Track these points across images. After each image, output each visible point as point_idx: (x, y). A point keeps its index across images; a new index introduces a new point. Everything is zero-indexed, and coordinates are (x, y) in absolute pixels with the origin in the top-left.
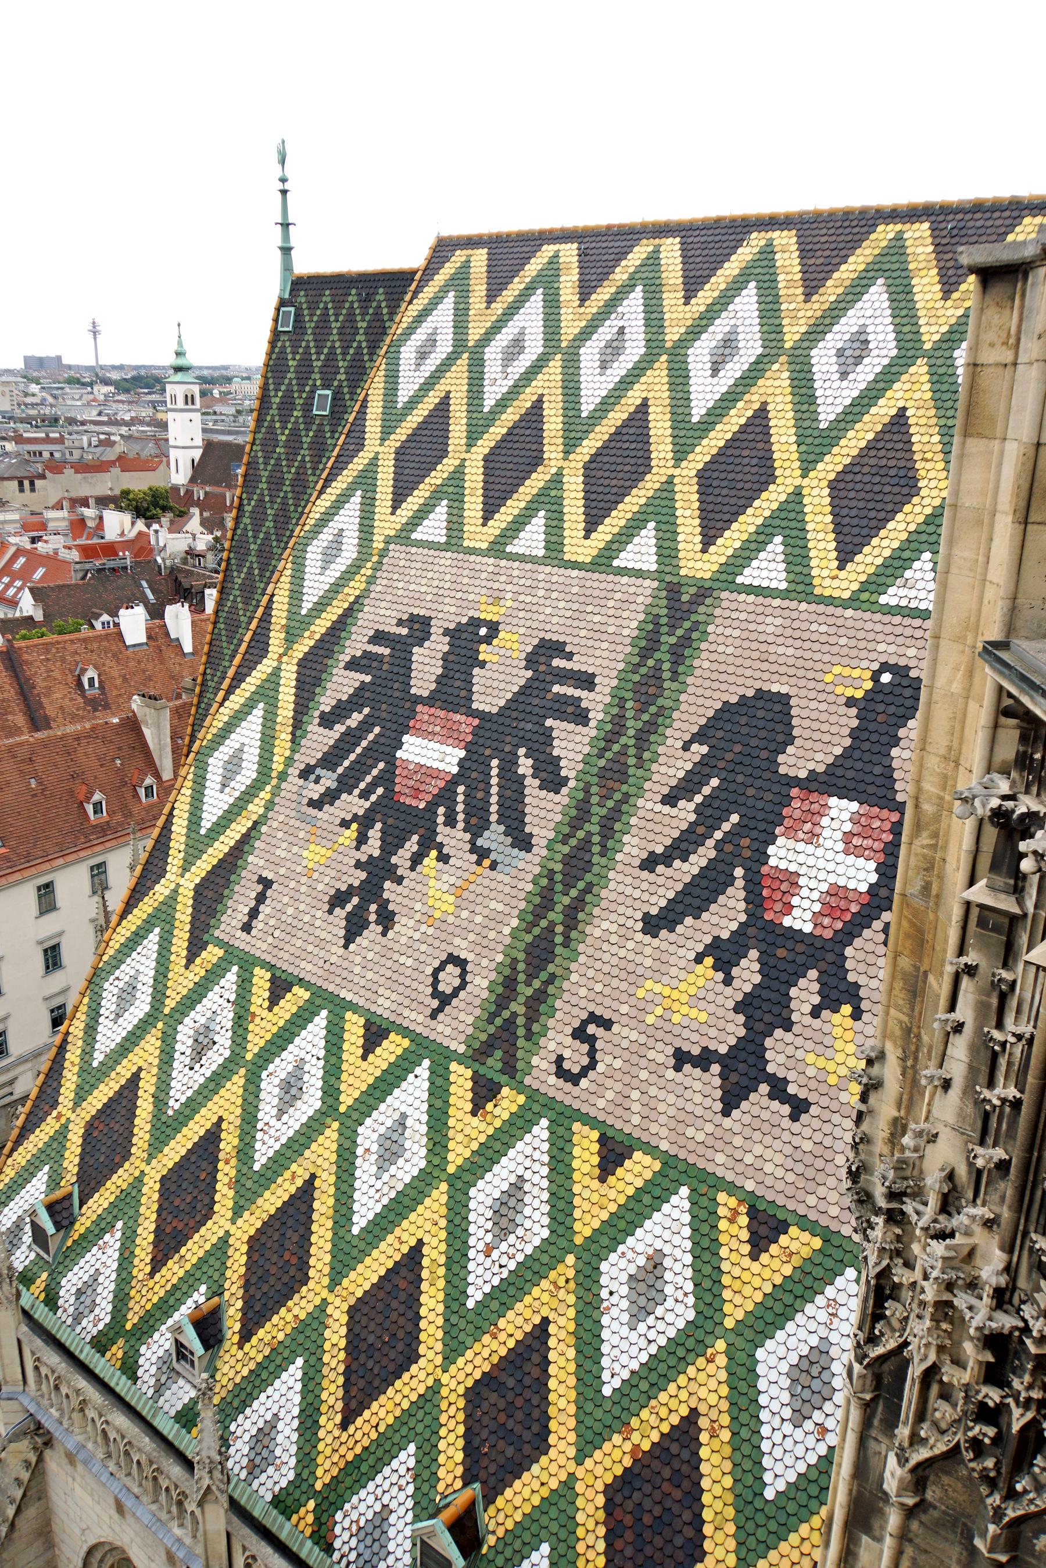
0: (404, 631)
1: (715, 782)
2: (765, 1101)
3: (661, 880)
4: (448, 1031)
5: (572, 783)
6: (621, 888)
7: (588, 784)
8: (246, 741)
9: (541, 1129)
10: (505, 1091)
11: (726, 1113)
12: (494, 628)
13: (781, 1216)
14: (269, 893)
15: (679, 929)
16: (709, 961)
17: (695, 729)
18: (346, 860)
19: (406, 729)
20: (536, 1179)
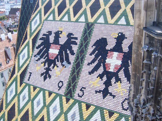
0: (48, 34)
1: (97, 51)
2: (109, 96)
3: (91, 67)
4: (61, 92)
5: (76, 54)
6: (85, 68)
7: (78, 54)
8: (25, 52)
9: (77, 104)
11: (104, 99)
12: (61, 32)
13: (113, 112)
14: (31, 75)
15: (94, 73)
16: (99, 77)
17: (93, 44)
18: (43, 68)
19: (50, 48)
20: (77, 112)
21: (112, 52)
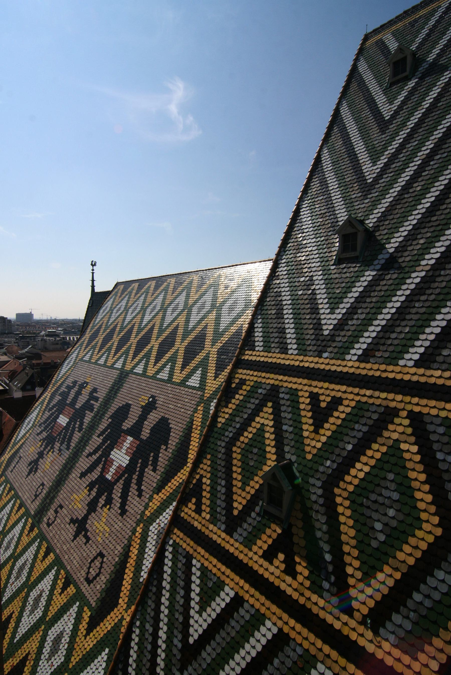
0: (72, 385)
10: (36, 529)
12: (87, 383)
21: (125, 436)
